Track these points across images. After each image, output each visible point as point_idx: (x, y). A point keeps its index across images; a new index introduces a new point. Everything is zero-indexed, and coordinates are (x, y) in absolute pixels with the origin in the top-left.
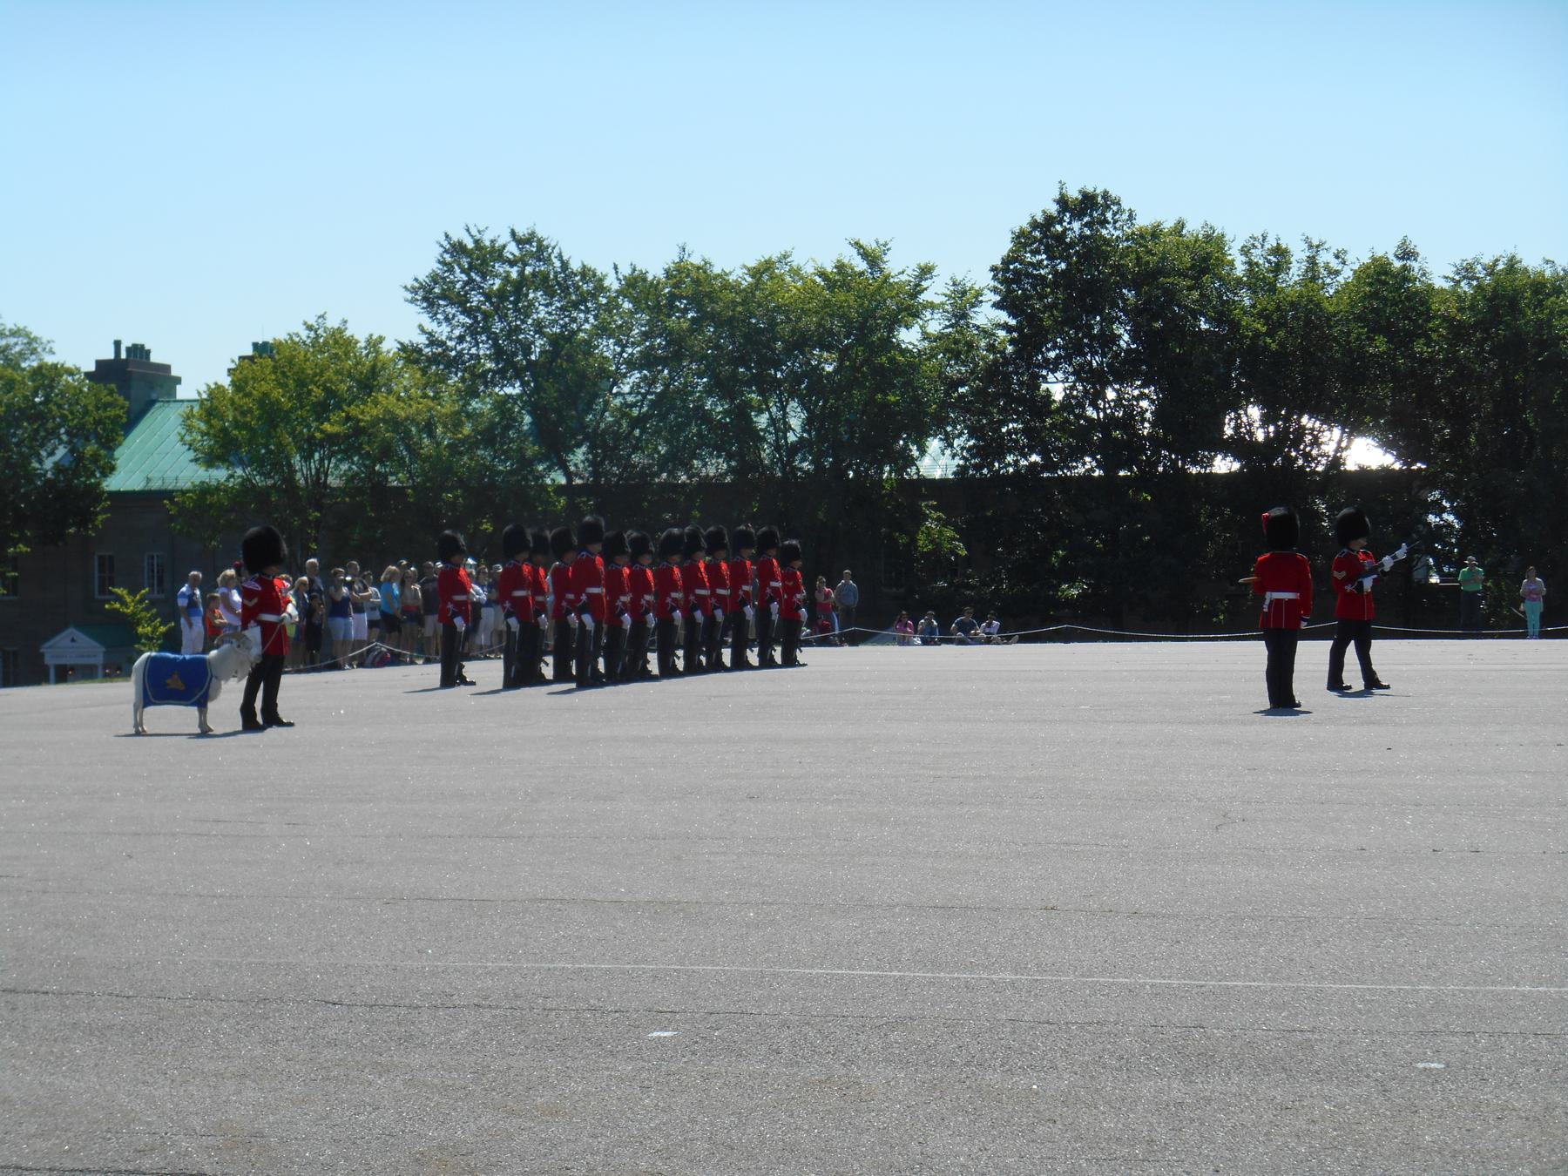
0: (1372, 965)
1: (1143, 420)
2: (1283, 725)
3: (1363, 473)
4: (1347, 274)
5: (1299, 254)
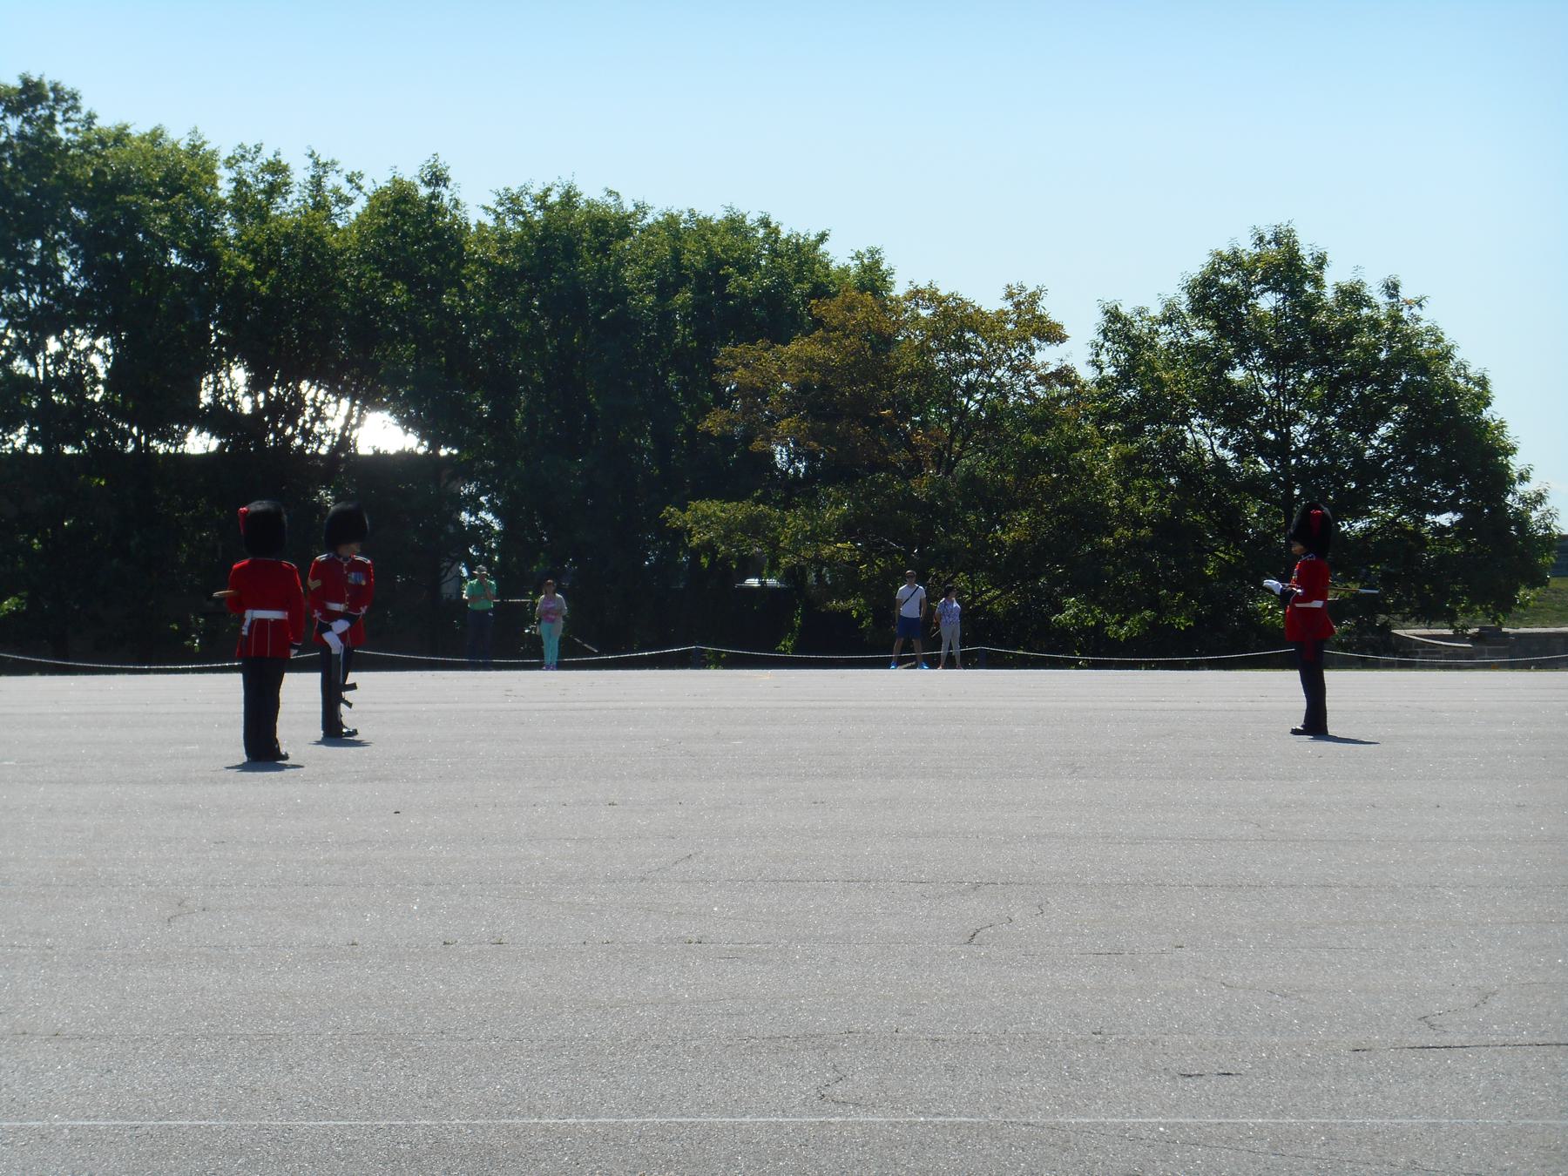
0: (357, 1094)
1: (96, 381)
2: (264, 782)
3: (379, 459)
4: (360, 205)
5: (300, 174)
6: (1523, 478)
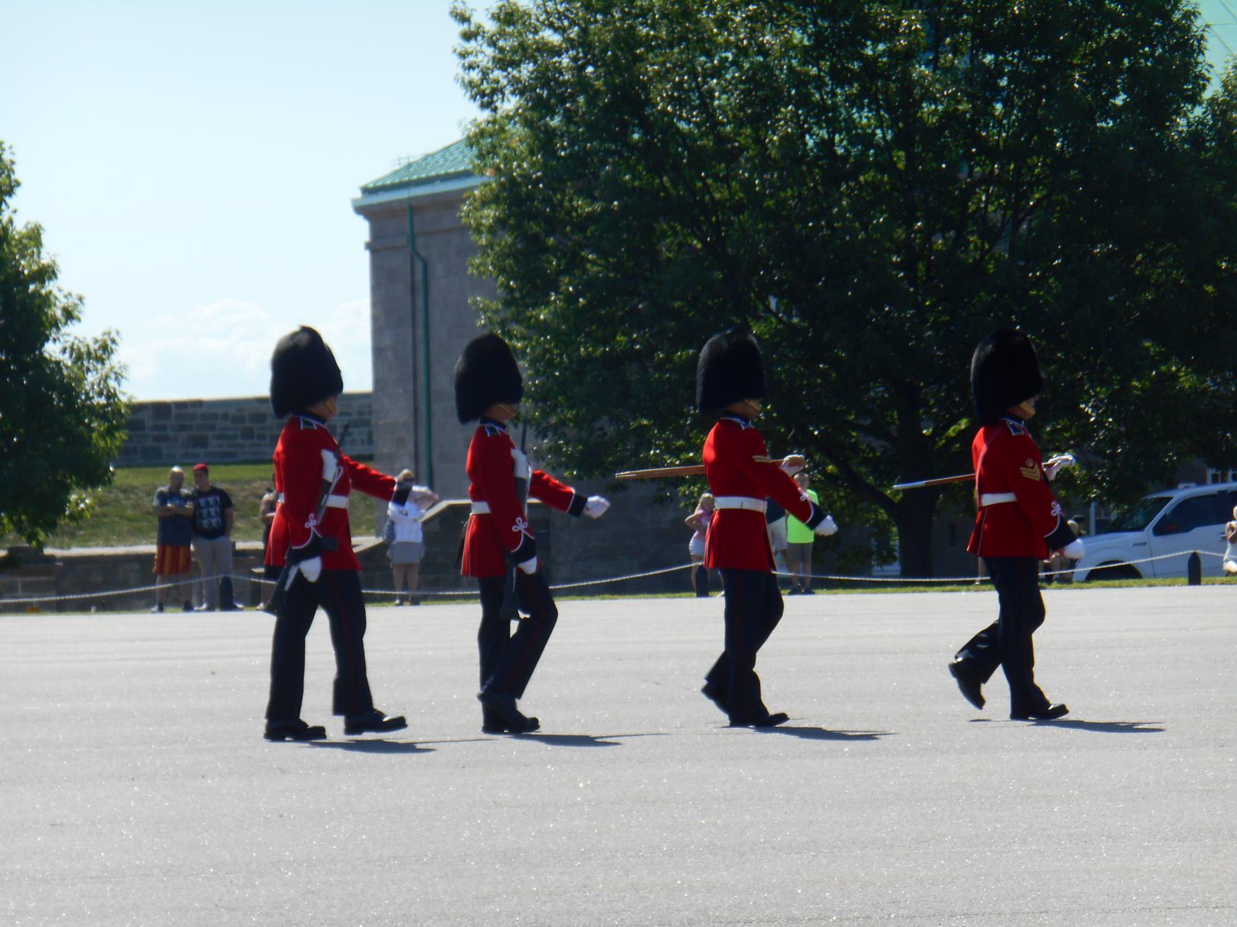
6: (69, 315)
